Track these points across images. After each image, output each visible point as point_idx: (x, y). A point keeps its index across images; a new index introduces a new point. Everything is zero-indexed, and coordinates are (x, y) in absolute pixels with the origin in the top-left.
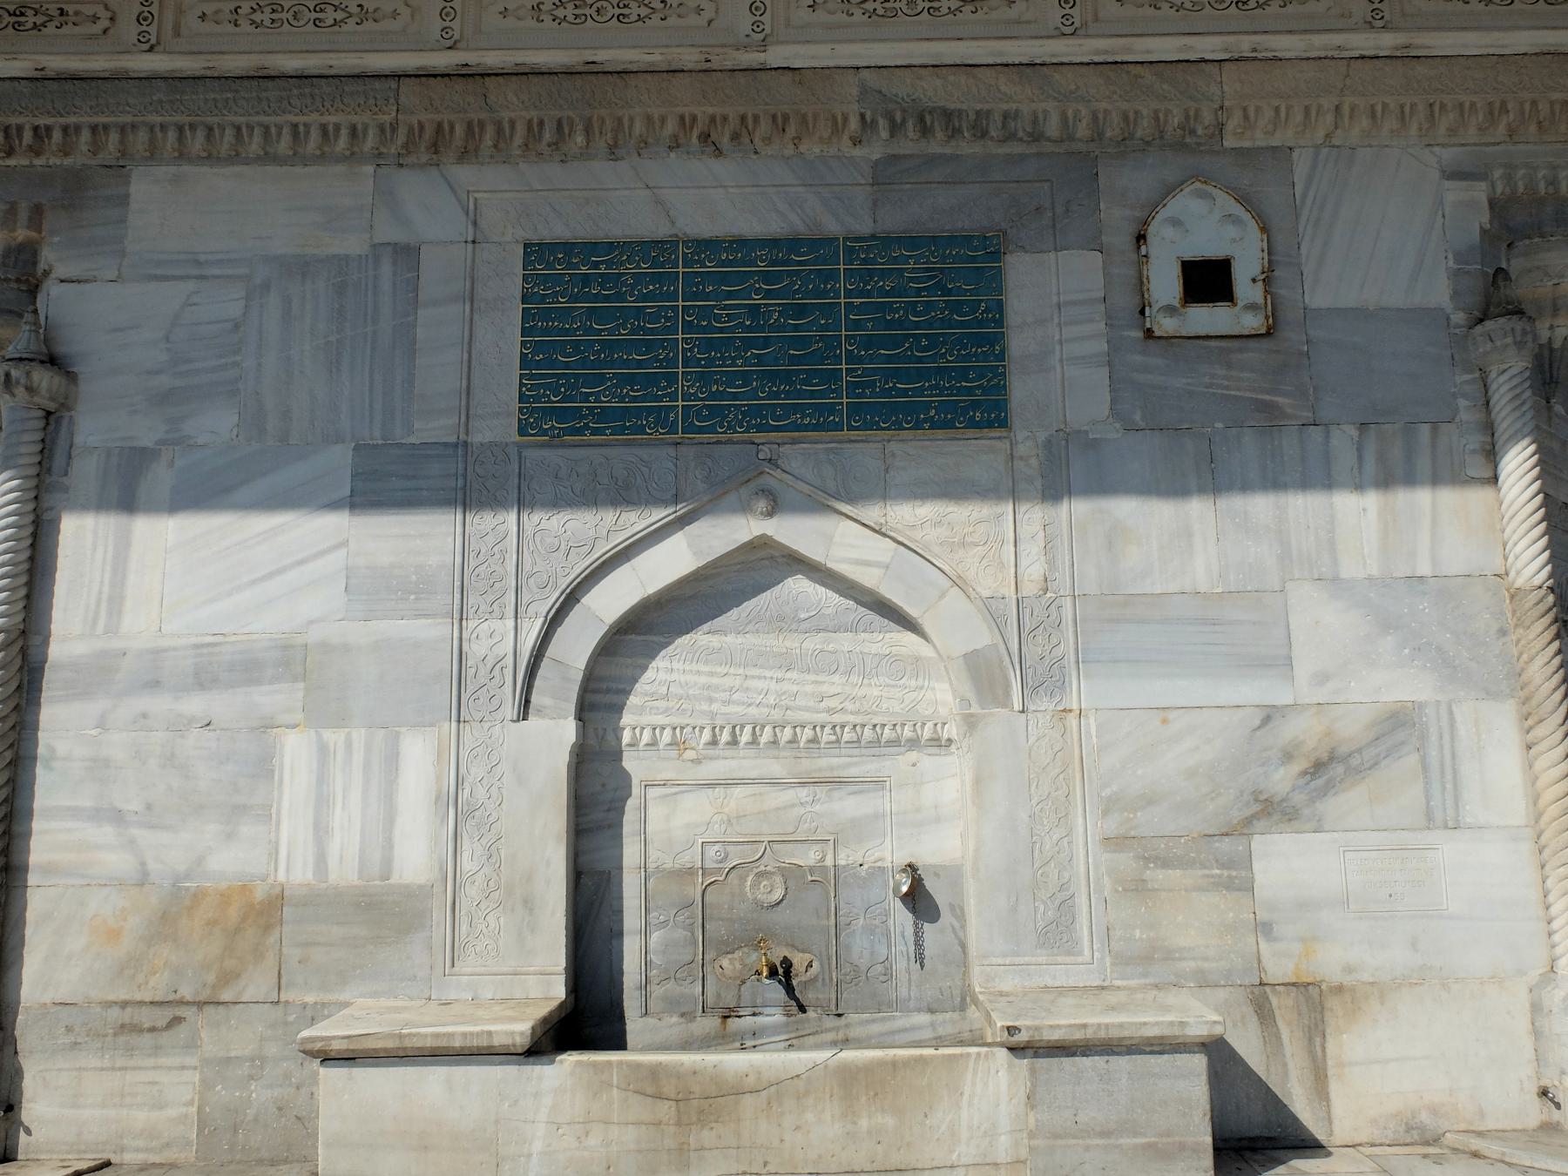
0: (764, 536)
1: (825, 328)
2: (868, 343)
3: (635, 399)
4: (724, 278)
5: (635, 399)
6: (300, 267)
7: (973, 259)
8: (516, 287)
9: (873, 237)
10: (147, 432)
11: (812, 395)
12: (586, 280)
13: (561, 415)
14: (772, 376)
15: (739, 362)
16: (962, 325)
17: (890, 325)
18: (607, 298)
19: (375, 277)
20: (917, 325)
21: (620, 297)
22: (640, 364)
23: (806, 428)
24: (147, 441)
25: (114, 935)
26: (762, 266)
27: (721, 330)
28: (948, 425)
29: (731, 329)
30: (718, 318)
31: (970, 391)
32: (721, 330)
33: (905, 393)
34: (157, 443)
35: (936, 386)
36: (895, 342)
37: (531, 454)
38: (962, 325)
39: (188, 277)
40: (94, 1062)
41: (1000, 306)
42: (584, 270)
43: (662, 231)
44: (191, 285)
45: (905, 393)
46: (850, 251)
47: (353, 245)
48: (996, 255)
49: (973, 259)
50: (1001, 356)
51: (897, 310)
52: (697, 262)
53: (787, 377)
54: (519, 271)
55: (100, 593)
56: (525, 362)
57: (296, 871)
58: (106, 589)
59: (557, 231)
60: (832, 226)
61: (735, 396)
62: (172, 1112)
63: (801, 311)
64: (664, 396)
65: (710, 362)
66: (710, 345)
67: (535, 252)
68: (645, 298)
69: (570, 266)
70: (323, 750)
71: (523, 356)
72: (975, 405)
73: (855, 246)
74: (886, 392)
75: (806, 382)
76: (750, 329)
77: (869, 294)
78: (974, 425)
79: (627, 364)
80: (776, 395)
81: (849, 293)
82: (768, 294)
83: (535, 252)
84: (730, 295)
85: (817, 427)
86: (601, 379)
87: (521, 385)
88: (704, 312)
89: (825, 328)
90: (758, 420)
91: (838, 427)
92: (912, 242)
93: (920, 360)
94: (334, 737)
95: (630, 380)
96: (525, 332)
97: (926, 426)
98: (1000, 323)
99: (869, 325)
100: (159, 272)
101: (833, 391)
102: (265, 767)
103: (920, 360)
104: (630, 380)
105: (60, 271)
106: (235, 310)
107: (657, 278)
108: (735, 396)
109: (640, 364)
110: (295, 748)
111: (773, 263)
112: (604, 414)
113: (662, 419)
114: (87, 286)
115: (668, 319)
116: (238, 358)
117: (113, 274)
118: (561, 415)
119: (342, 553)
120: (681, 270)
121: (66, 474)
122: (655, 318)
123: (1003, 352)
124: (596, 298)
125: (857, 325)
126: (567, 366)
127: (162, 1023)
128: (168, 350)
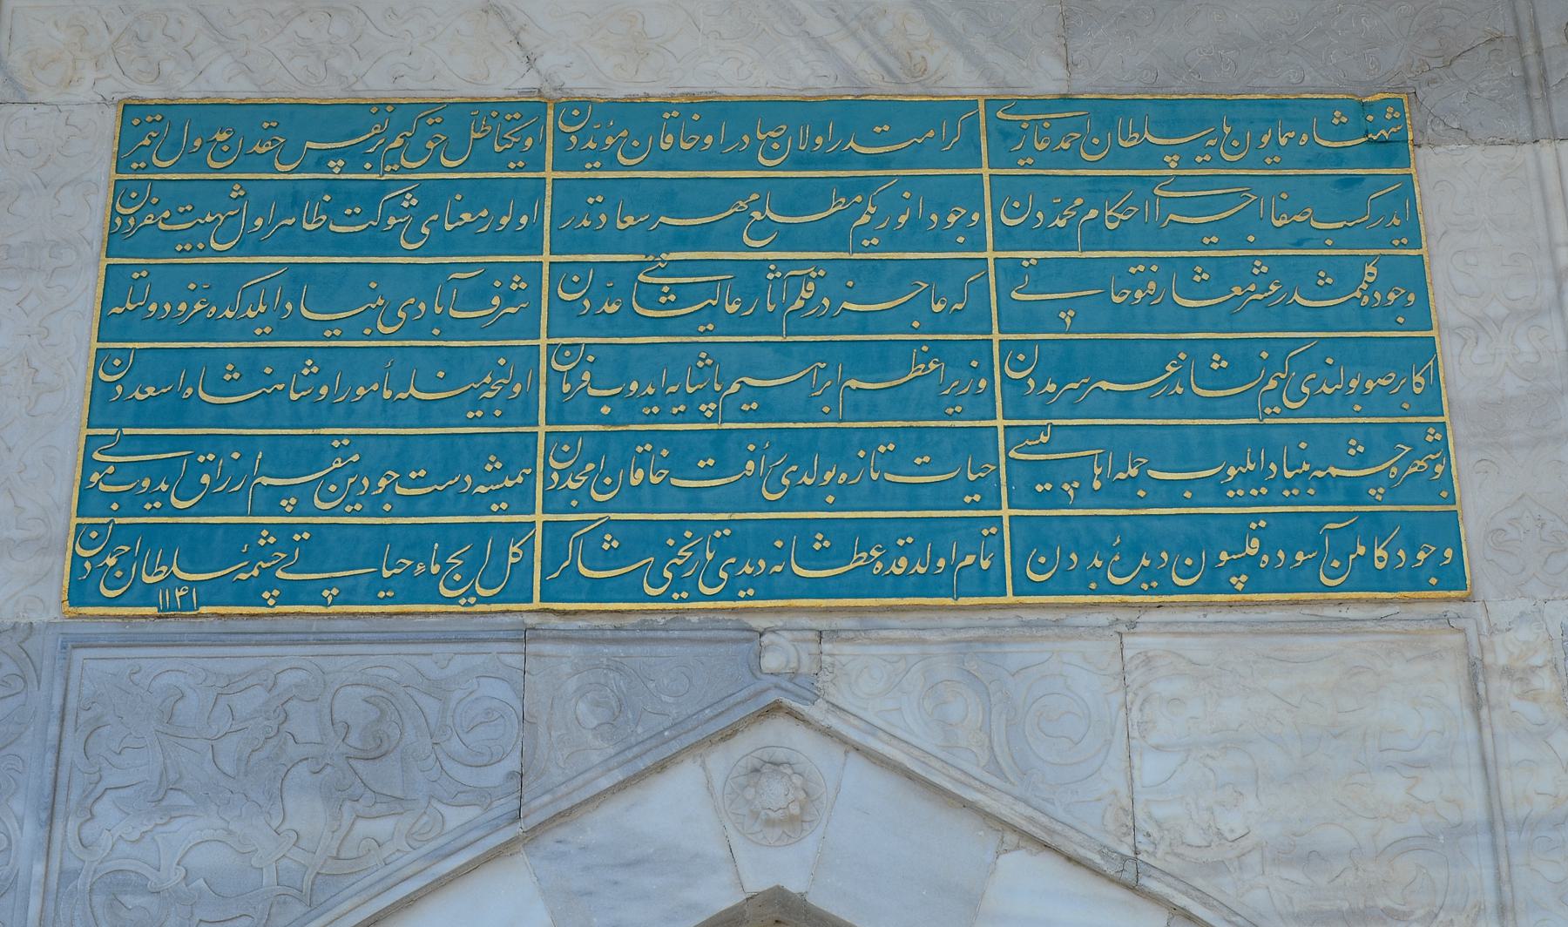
0: (778, 897)
1: (949, 321)
2: (1066, 363)
3: (410, 505)
4: (670, 198)
5: (410, 505)
7: (1338, 158)
8: (90, 215)
9: (1066, 100)
11: (913, 497)
12: (294, 199)
13: (196, 546)
14: (799, 449)
15: (708, 409)
16: (1317, 319)
17: (1123, 317)
18: (343, 244)
20: (1194, 319)
21: (382, 242)
22: (425, 414)
23: (898, 586)
26: (770, 168)
27: (658, 326)
28: (1292, 580)
29: (686, 325)
30: (650, 296)
31: (1354, 491)
32: (658, 326)
33: (1171, 494)
35: (1257, 478)
36: (1125, 362)
37: (97, 669)
38: (1317, 319)
41: (1415, 276)
42: (284, 172)
43: (505, 80)
45: (1171, 494)
46: (1005, 135)
48: (1393, 149)
49: (1338, 158)
50: (1432, 401)
51: (1138, 282)
52: (595, 154)
53: (839, 447)
54: (103, 171)
56: (102, 404)
59: (221, 79)
60: (958, 77)
61: (694, 500)
63: (869, 277)
64: (494, 496)
65: (629, 406)
66: (619, 365)
67: (148, 128)
68: (445, 243)
69: (247, 160)
71: (100, 393)
72: (1375, 527)
73: (1010, 123)
74: (1116, 491)
75: (892, 463)
76: (736, 324)
77: (1062, 240)
78: (1369, 579)
79: (389, 412)
80: (811, 498)
81: (1005, 237)
82: (786, 238)
83: (148, 128)
84: (683, 239)
85: (924, 586)
86: (314, 453)
87: (89, 464)
88: (612, 281)
89: (949, 321)
90: (761, 563)
91: (988, 583)
92: (1175, 115)
93: (1207, 408)
95: (401, 455)
96: (107, 326)
97: (1239, 582)
98: (1422, 315)
99: (1067, 317)
101: (972, 488)
103: (1207, 408)
104: (401, 455)
107: (476, 194)
108: (694, 500)
109: (425, 414)
111: (799, 162)
112: (320, 547)
113: (486, 559)
115: (509, 297)
118: (196, 546)
120: (549, 174)
122: (477, 294)
123: (1434, 385)
124: (316, 242)
125: (1031, 318)
126: (222, 416)
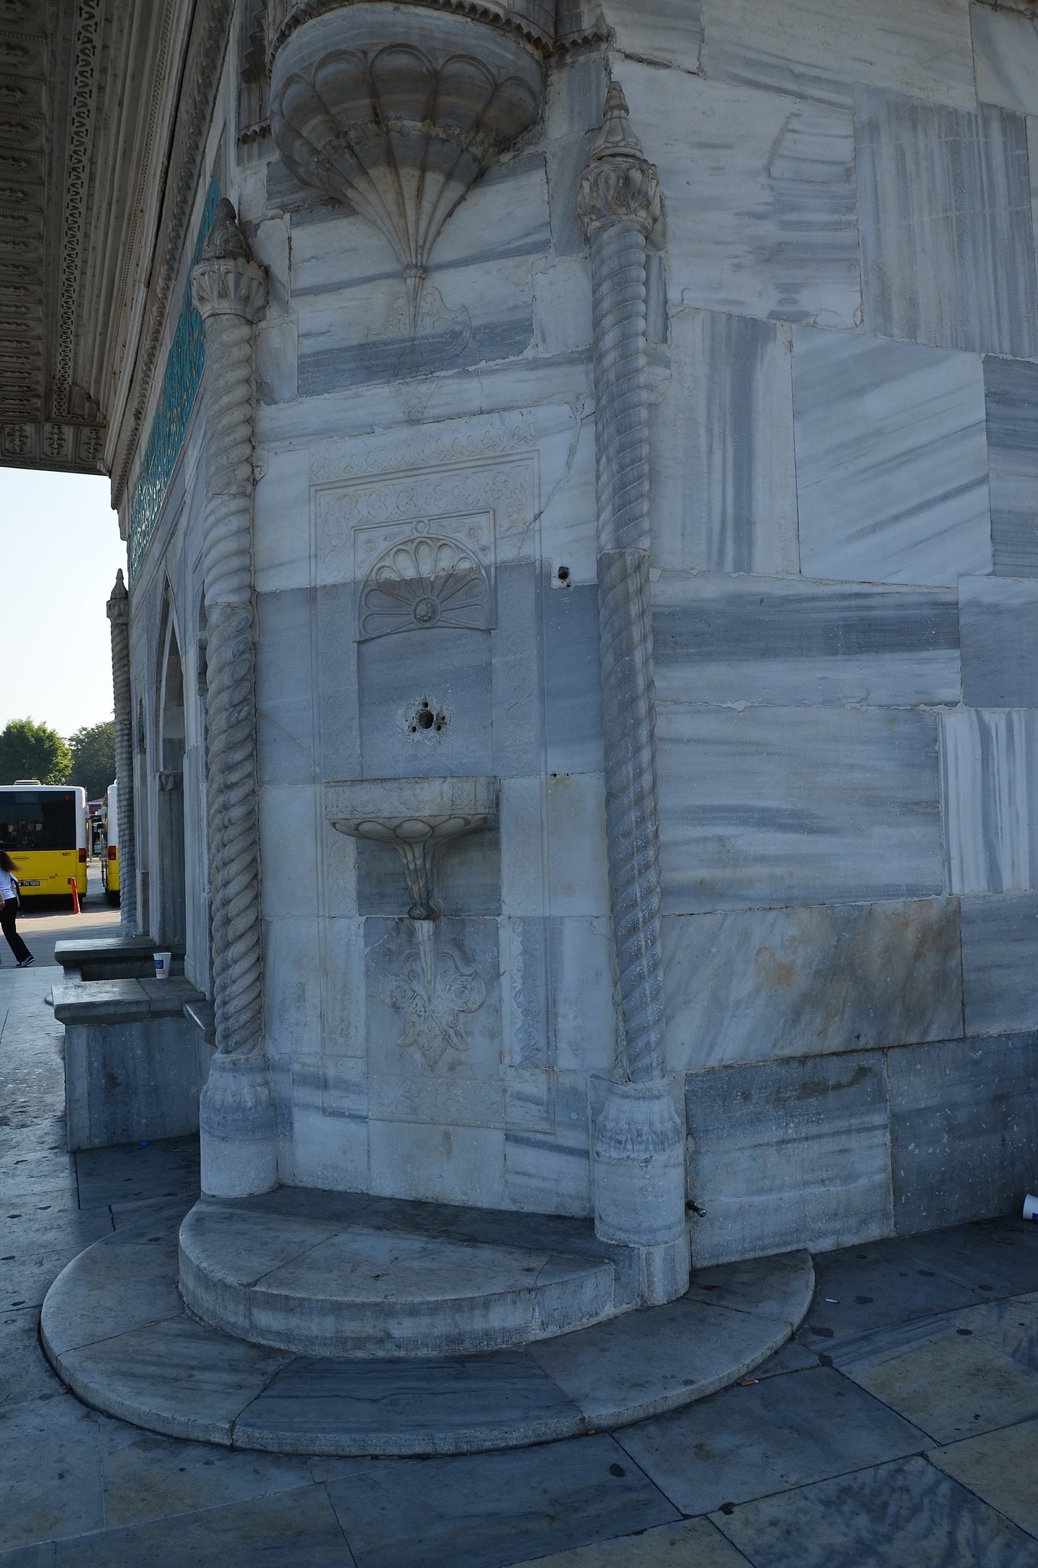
6: (911, 113)
10: (758, 299)
19: (986, 143)
24: (759, 309)
25: (786, 972)
34: (772, 315)
39: (786, 92)
40: (775, 1134)
44: (789, 104)
47: (959, 97)
55: (724, 514)
57: (968, 883)
58: (730, 511)
62: (863, 1182)
70: (985, 734)
94: (995, 718)
100: (749, 75)
102: (926, 753)
105: (626, 39)
106: (844, 150)
110: (958, 729)
114: (662, 72)
116: (852, 217)
117: (692, 64)
119: (983, 491)
121: (665, 340)
127: (846, 1078)
128: (772, 188)
